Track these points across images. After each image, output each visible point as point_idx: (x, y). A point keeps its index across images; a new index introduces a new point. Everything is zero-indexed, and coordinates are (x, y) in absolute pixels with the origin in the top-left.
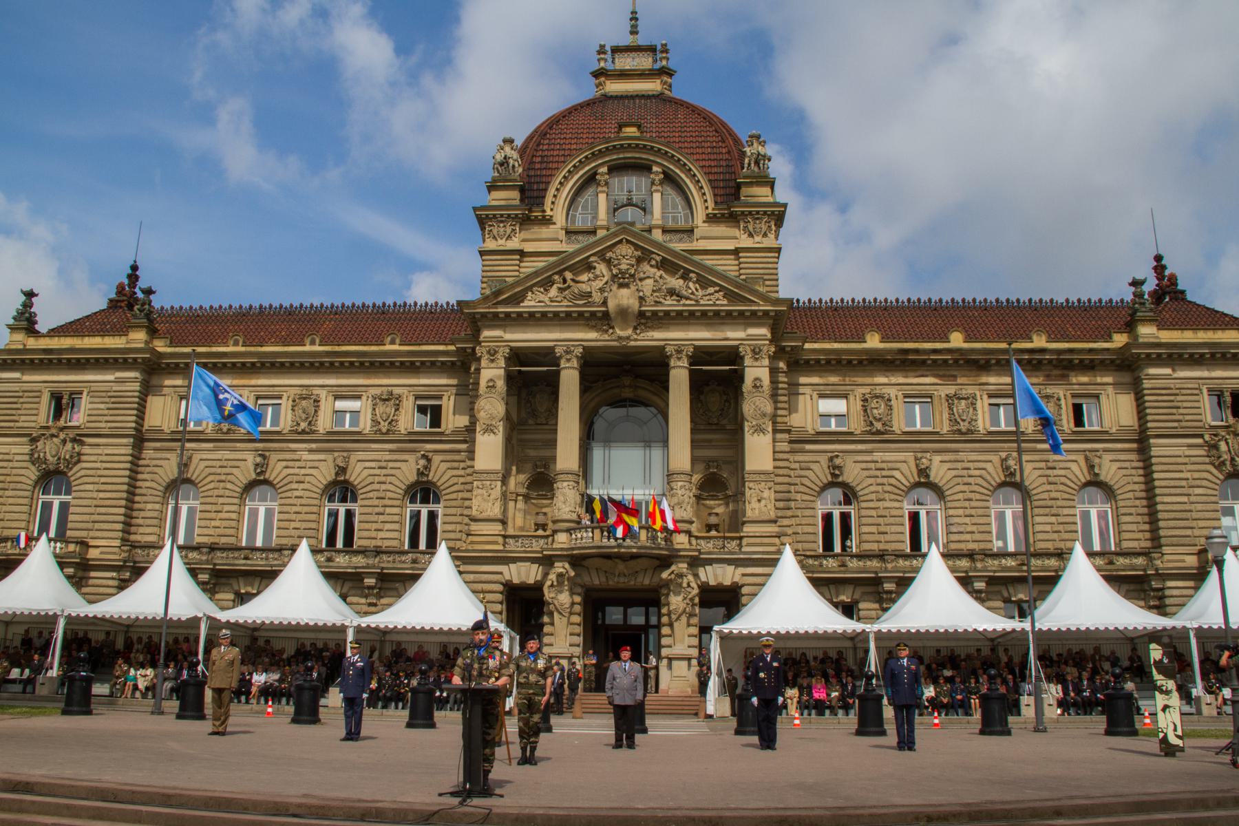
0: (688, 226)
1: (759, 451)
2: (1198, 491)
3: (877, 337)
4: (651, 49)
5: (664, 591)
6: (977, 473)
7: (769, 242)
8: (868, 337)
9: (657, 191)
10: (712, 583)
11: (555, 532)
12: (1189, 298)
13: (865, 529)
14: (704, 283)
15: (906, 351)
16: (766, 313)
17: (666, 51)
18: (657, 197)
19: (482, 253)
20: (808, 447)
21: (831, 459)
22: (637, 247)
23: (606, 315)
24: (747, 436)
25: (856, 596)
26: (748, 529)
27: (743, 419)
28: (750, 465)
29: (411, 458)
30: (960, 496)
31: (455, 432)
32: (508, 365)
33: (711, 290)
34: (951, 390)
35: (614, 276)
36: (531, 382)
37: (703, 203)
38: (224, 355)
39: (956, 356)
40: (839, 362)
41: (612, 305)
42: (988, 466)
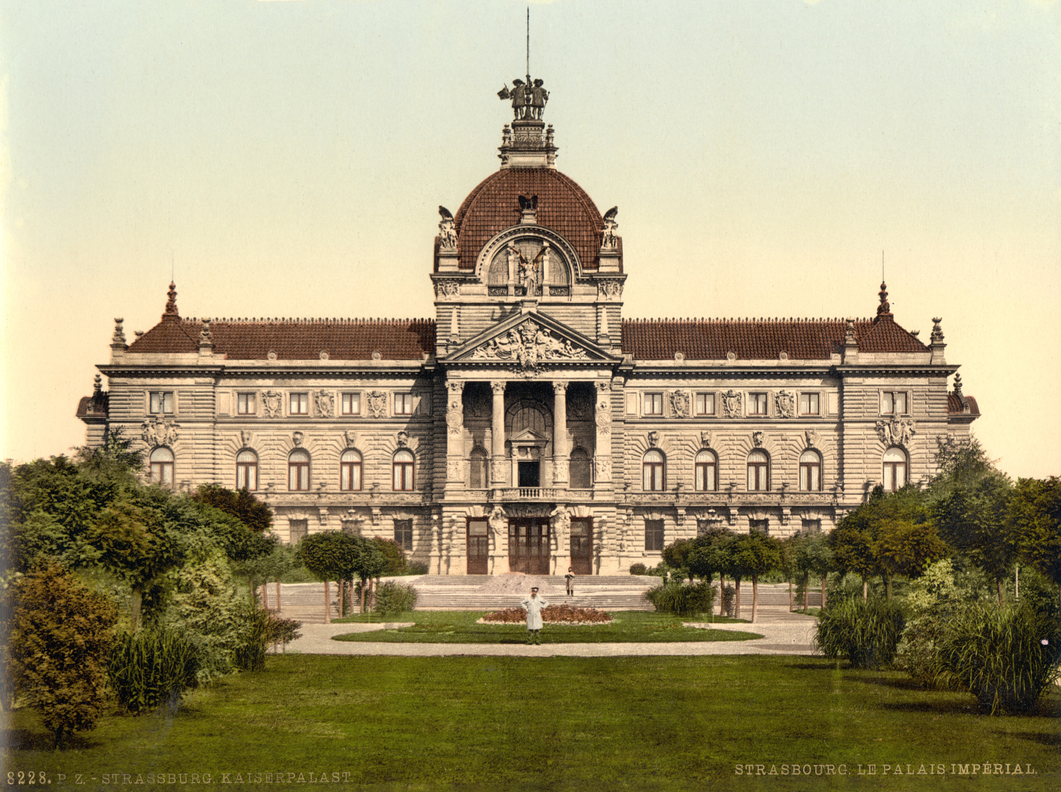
2: (869, 456)
5: (551, 520)
7: (616, 299)
10: (578, 516)
12: (896, 320)
16: (609, 364)
17: (550, 131)
19: (436, 304)
21: (650, 434)
22: (536, 323)
26: (597, 487)
27: (595, 425)
30: (727, 457)
33: (579, 350)
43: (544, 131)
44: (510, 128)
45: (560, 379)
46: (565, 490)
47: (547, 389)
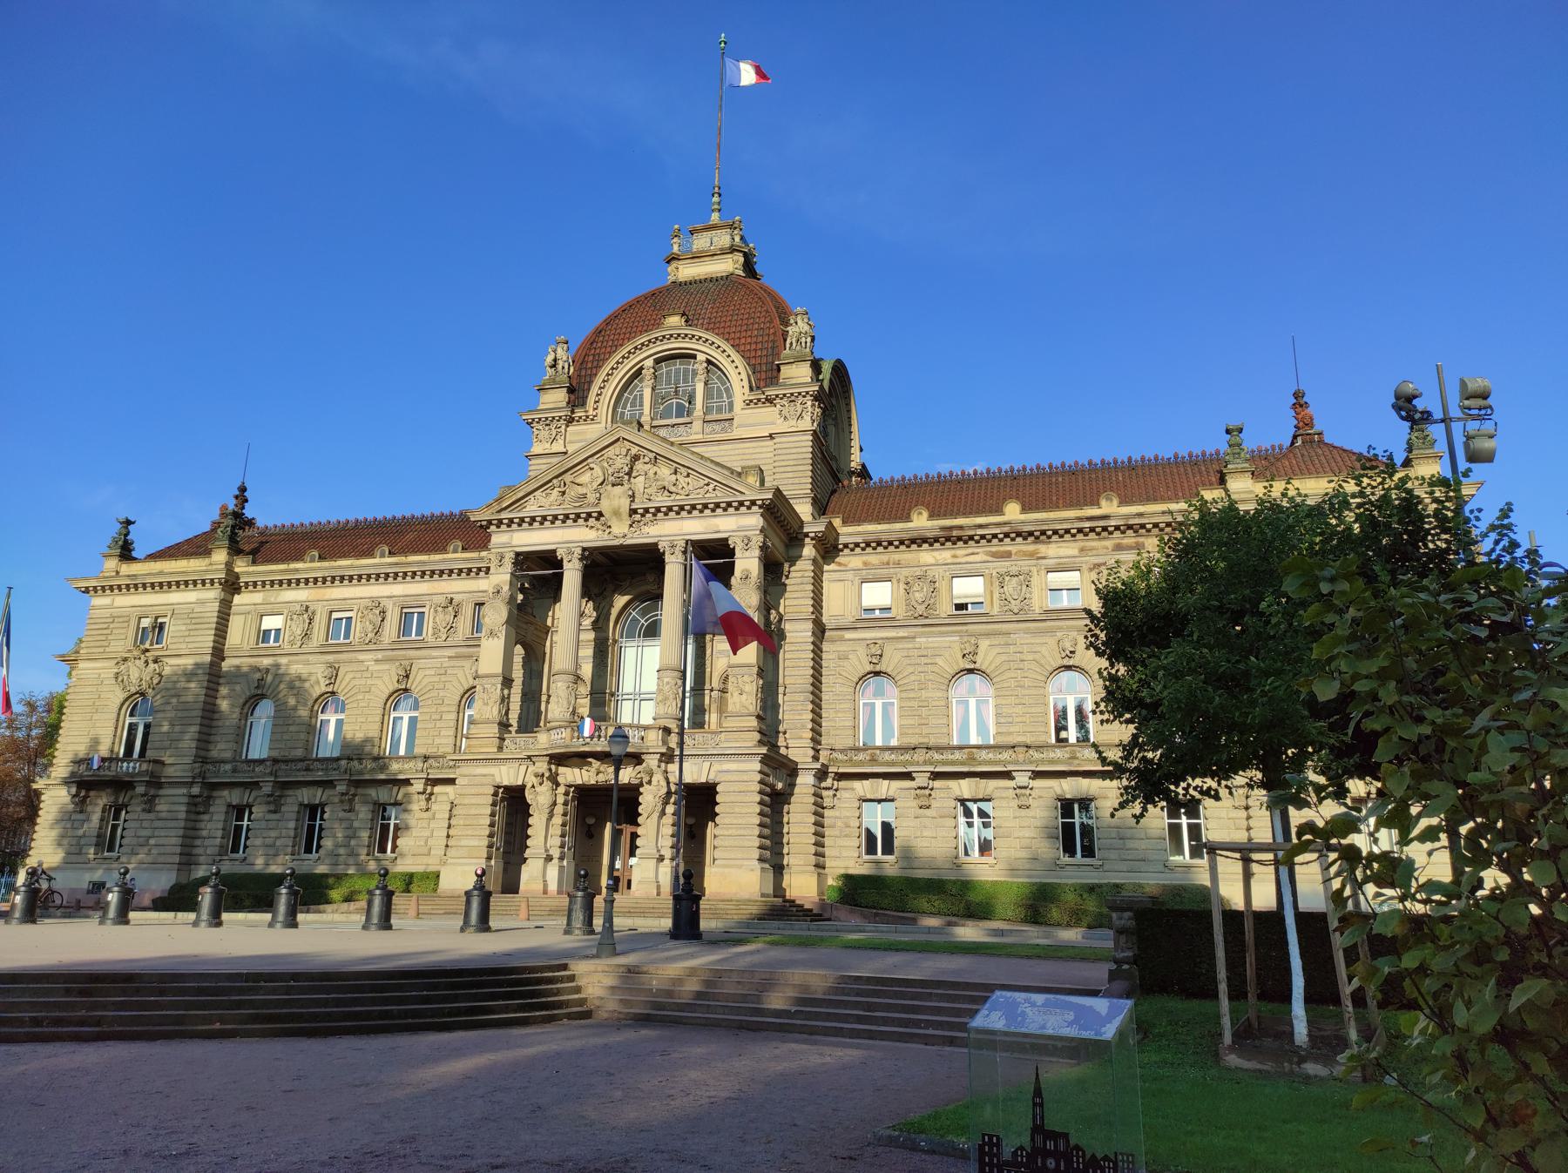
0: (728, 416)
3: (925, 514)
6: (1030, 657)
8: (914, 516)
15: (951, 528)
20: (848, 635)
23: (600, 514)
34: (1002, 566)
38: (297, 570)
39: (1006, 529)
41: (605, 506)
42: (1044, 650)
45: (671, 533)
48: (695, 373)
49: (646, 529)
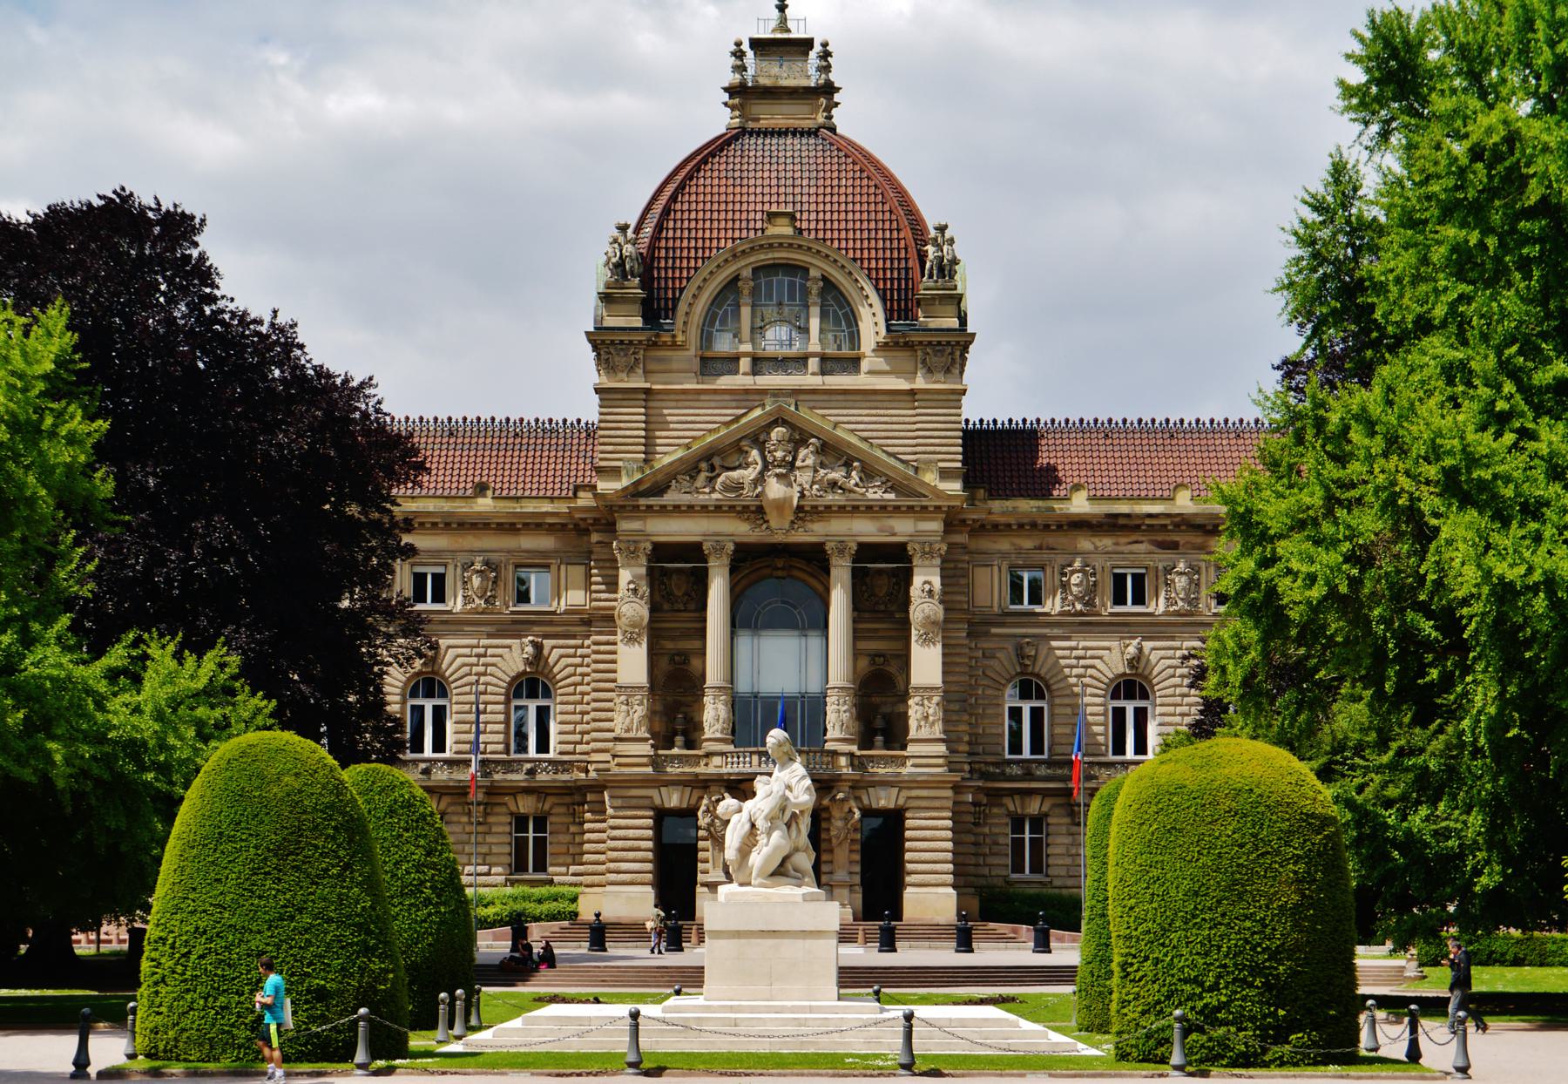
1: (926, 664)
4: (807, 44)
9: (815, 304)
11: (708, 755)
13: (1058, 730)
14: (868, 473)
16: (938, 508)
17: (826, 55)
18: (815, 311)
19: (597, 391)
20: (994, 630)
24: (914, 645)
25: (1045, 808)
26: (912, 749)
28: (916, 679)
29: (514, 642)
31: (566, 612)
32: (649, 561)
35: (766, 467)
36: (676, 577)
37: (872, 323)
40: (1034, 525)
43: (813, 54)
44: (746, 47)
46: (851, 755)
47: (815, 559)
48: (805, 292)
49: (810, 526)
